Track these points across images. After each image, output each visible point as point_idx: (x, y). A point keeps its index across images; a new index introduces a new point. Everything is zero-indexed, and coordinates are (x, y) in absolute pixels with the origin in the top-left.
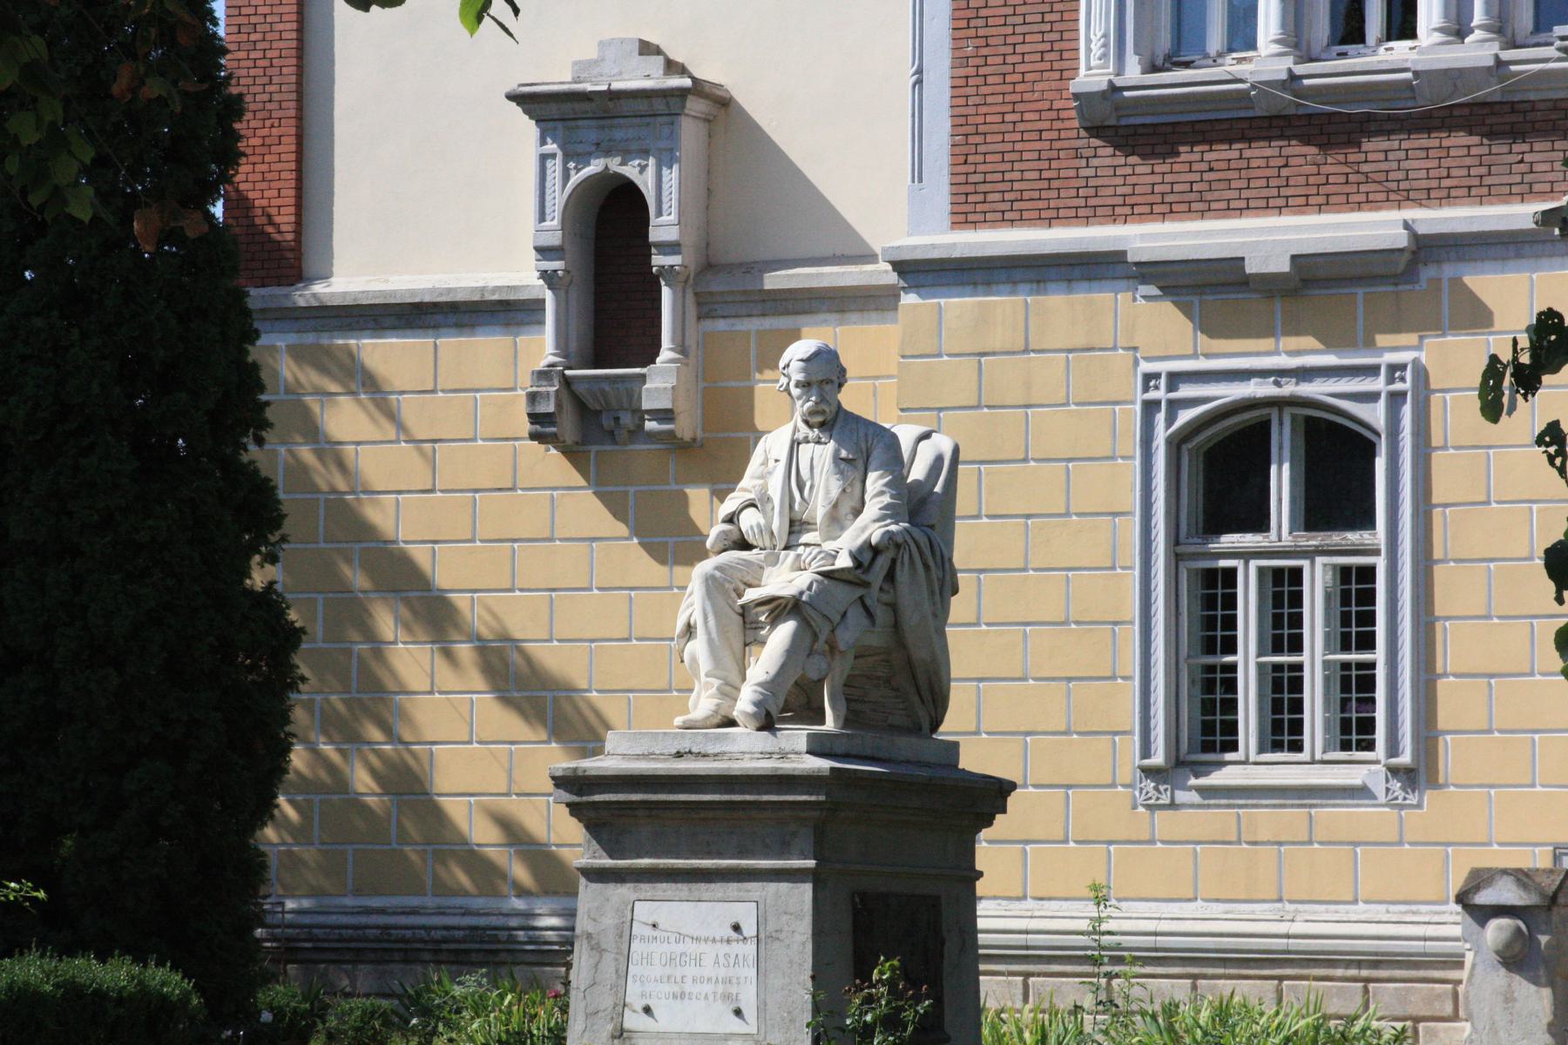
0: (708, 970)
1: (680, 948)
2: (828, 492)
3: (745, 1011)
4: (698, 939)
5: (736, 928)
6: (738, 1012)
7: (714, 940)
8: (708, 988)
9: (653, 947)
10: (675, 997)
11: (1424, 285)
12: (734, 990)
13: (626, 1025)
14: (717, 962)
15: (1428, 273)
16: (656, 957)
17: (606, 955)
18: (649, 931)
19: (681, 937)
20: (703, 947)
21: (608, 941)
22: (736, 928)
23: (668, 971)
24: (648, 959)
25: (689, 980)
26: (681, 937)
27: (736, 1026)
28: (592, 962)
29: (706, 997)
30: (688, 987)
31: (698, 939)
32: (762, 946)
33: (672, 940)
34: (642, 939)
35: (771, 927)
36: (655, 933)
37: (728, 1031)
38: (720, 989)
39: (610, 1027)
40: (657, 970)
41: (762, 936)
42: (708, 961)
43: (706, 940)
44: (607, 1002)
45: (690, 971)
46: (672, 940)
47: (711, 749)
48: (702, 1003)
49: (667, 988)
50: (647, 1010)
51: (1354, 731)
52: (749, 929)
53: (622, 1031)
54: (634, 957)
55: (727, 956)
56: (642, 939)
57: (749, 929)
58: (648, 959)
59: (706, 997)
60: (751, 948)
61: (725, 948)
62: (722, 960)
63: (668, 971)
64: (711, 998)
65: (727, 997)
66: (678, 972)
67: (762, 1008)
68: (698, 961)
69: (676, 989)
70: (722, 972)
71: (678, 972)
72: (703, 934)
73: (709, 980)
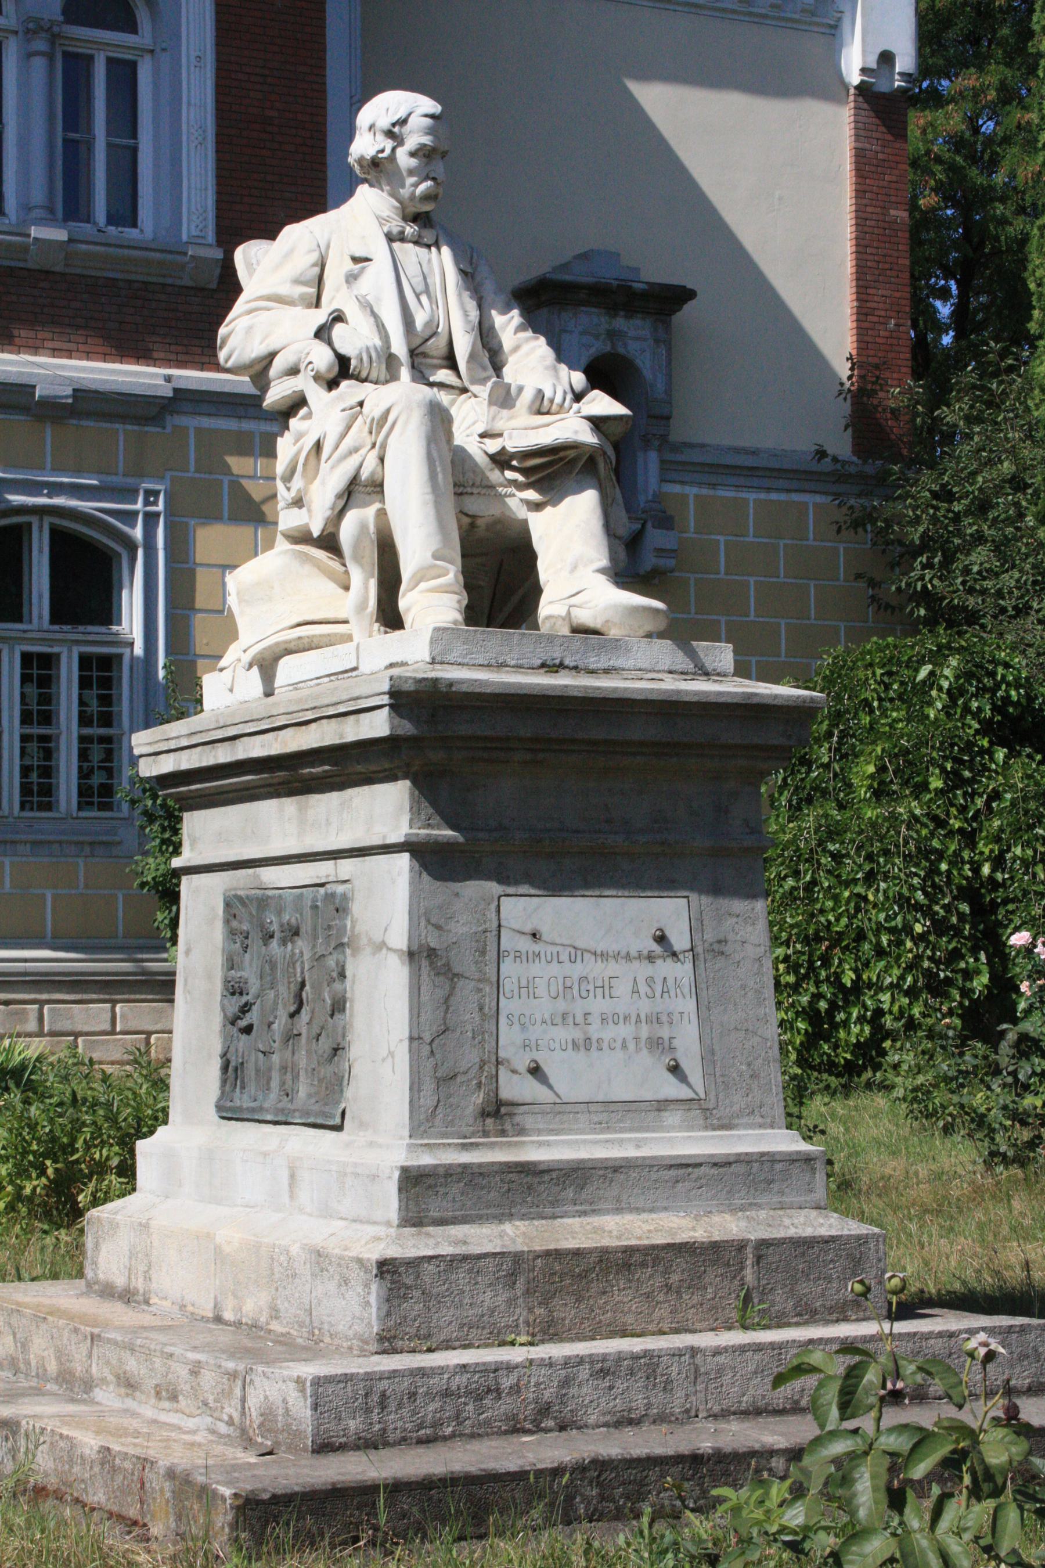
0: (623, 1001)
1: (577, 970)
2: (466, 314)
3: (684, 1065)
4: (604, 956)
5: (661, 939)
6: (675, 1069)
7: (628, 957)
8: (625, 1031)
9: (536, 969)
10: (575, 1045)
12: (665, 1033)
13: (505, 1094)
14: (635, 991)
16: (541, 991)
17: (461, 983)
18: (525, 944)
19: (577, 953)
20: (613, 968)
21: (464, 962)
23: (561, 1005)
24: (528, 988)
26: (577, 953)
27: (672, 1089)
28: (440, 993)
29: (624, 1046)
30: (595, 1030)
31: (604, 956)
32: (701, 965)
33: (564, 957)
34: (518, 956)
35: (709, 936)
36: (537, 947)
37: (661, 1096)
38: (645, 1032)
39: (478, 1099)
40: (544, 1007)
41: (699, 949)
42: (622, 988)
43: (617, 956)
44: (470, 1057)
45: (598, 1005)
46: (564, 957)
47: (593, 662)
48: (619, 1054)
49: (563, 1034)
50: (536, 1071)
53: (500, 1103)
54: (507, 985)
55: (650, 981)
56: (518, 956)
57: (680, 941)
58: (528, 988)
59: (624, 1046)
60: (682, 971)
61: (643, 970)
62: (643, 988)
64: (631, 1046)
65: (656, 1044)
66: (578, 1008)
67: (708, 1057)
68: (607, 988)
69: (577, 1034)
70: (645, 1007)
72: (614, 947)
73: (626, 1018)
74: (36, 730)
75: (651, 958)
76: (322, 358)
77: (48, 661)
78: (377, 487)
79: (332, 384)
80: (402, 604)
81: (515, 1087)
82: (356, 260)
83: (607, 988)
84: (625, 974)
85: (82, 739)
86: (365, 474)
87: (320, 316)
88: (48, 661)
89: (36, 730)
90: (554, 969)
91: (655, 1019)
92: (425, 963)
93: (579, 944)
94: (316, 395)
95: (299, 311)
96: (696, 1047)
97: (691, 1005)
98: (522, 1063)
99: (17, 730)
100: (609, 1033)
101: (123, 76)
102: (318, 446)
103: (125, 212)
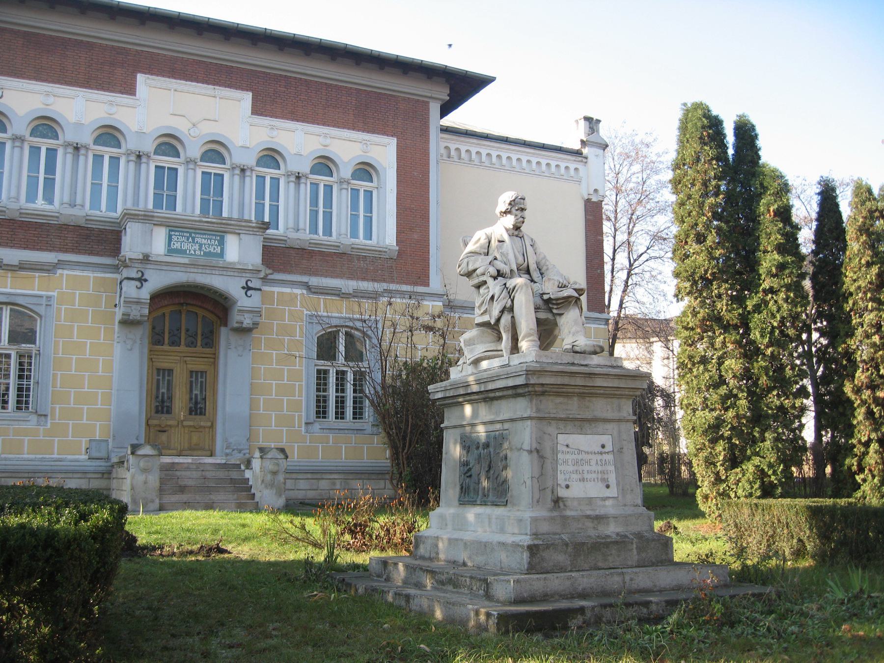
0: (594, 468)
1: (580, 457)
4: (588, 453)
6: (608, 487)
8: (594, 476)
11: (58, 275)
12: (606, 476)
13: (560, 495)
14: (597, 463)
15: (59, 271)
16: (570, 461)
18: (565, 449)
20: (590, 456)
22: (603, 446)
25: (585, 472)
26: (580, 452)
30: (586, 476)
31: (588, 453)
36: (568, 450)
38: (600, 476)
40: (571, 468)
42: (593, 462)
45: (586, 468)
49: (574, 476)
51: (22, 403)
52: (609, 447)
58: (566, 462)
60: (610, 457)
61: (599, 457)
63: (575, 468)
65: (603, 480)
66: (580, 468)
69: (580, 476)
70: (600, 468)
71: (580, 468)
72: (590, 450)
74: (340, 394)
75: (601, 453)
76: (492, 271)
77: (344, 373)
78: (511, 309)
79: (495, 278)
80: (519, 345)
81: (562, 493)
82: (499, 241)
83: (588, 462)
84: (594, 458)
85: (354, 397)
86: (508, 305)
87: (490, 258)
88: (344, 373)
89: (340, 394)
90: (574, 457)
91: (603, 472)
92: (535, 454)
93: (581, 448)
94: (490, 282)
95: (483, 257)
96: (615, 481)
97: (612, 468)
98: (563, 484)
99: (335, 394)
100: (589, 476)
101: (369, 194)
102: (492, 297)
103: (369, 235)
